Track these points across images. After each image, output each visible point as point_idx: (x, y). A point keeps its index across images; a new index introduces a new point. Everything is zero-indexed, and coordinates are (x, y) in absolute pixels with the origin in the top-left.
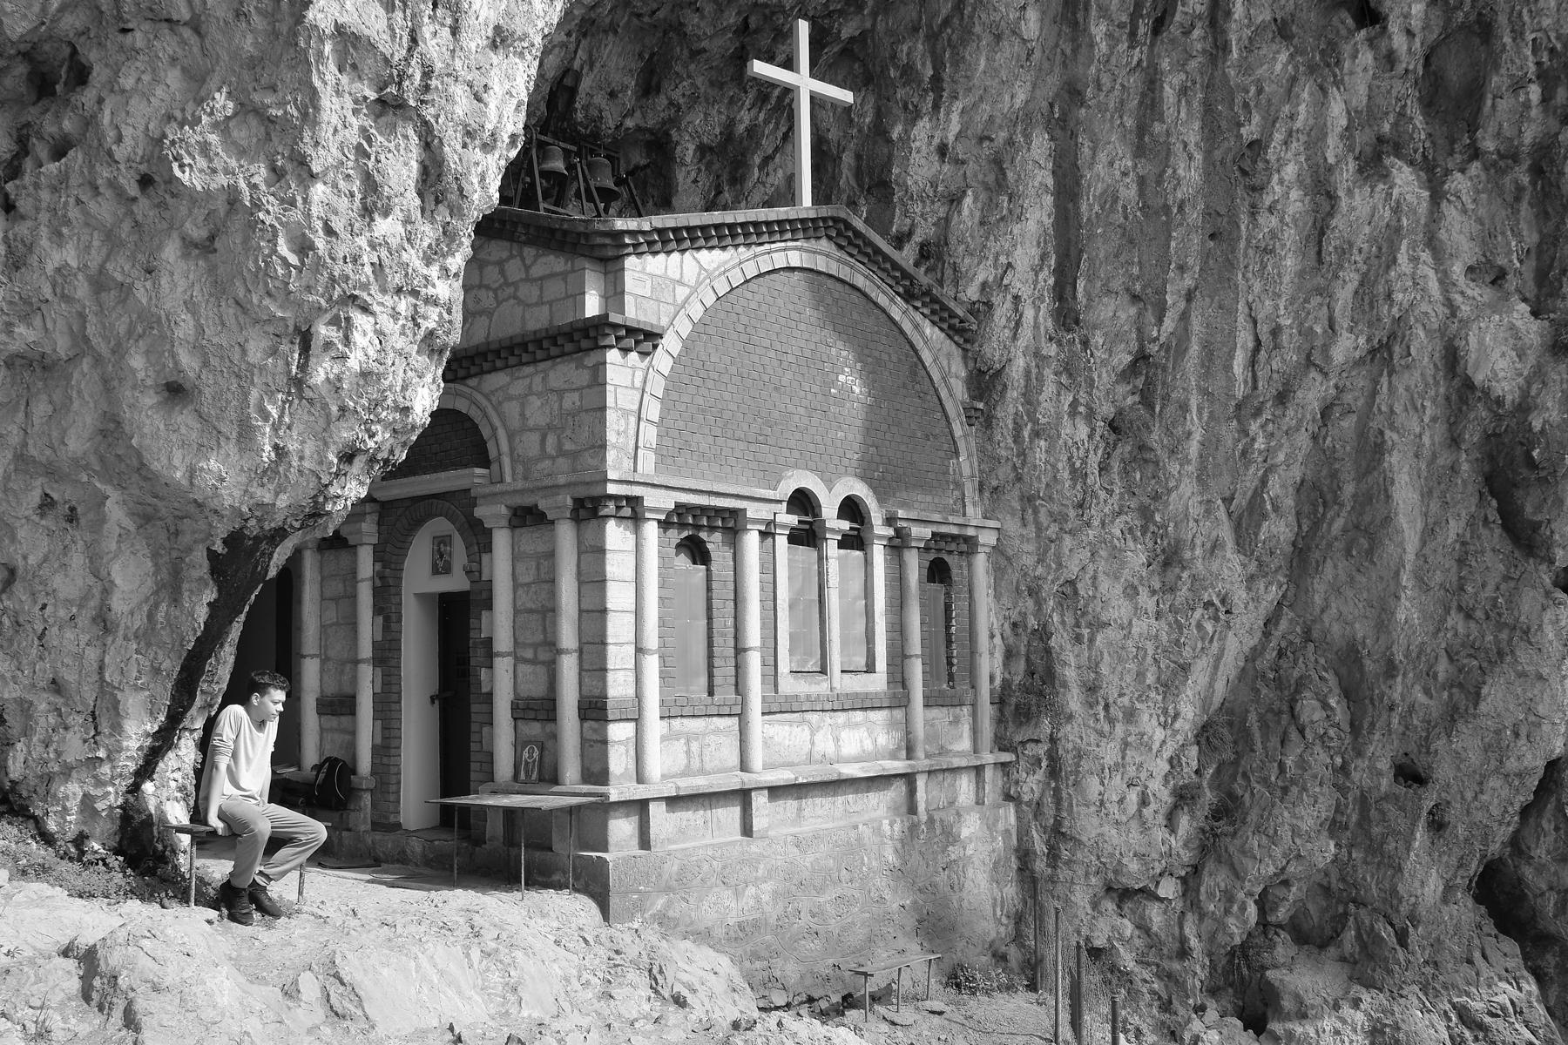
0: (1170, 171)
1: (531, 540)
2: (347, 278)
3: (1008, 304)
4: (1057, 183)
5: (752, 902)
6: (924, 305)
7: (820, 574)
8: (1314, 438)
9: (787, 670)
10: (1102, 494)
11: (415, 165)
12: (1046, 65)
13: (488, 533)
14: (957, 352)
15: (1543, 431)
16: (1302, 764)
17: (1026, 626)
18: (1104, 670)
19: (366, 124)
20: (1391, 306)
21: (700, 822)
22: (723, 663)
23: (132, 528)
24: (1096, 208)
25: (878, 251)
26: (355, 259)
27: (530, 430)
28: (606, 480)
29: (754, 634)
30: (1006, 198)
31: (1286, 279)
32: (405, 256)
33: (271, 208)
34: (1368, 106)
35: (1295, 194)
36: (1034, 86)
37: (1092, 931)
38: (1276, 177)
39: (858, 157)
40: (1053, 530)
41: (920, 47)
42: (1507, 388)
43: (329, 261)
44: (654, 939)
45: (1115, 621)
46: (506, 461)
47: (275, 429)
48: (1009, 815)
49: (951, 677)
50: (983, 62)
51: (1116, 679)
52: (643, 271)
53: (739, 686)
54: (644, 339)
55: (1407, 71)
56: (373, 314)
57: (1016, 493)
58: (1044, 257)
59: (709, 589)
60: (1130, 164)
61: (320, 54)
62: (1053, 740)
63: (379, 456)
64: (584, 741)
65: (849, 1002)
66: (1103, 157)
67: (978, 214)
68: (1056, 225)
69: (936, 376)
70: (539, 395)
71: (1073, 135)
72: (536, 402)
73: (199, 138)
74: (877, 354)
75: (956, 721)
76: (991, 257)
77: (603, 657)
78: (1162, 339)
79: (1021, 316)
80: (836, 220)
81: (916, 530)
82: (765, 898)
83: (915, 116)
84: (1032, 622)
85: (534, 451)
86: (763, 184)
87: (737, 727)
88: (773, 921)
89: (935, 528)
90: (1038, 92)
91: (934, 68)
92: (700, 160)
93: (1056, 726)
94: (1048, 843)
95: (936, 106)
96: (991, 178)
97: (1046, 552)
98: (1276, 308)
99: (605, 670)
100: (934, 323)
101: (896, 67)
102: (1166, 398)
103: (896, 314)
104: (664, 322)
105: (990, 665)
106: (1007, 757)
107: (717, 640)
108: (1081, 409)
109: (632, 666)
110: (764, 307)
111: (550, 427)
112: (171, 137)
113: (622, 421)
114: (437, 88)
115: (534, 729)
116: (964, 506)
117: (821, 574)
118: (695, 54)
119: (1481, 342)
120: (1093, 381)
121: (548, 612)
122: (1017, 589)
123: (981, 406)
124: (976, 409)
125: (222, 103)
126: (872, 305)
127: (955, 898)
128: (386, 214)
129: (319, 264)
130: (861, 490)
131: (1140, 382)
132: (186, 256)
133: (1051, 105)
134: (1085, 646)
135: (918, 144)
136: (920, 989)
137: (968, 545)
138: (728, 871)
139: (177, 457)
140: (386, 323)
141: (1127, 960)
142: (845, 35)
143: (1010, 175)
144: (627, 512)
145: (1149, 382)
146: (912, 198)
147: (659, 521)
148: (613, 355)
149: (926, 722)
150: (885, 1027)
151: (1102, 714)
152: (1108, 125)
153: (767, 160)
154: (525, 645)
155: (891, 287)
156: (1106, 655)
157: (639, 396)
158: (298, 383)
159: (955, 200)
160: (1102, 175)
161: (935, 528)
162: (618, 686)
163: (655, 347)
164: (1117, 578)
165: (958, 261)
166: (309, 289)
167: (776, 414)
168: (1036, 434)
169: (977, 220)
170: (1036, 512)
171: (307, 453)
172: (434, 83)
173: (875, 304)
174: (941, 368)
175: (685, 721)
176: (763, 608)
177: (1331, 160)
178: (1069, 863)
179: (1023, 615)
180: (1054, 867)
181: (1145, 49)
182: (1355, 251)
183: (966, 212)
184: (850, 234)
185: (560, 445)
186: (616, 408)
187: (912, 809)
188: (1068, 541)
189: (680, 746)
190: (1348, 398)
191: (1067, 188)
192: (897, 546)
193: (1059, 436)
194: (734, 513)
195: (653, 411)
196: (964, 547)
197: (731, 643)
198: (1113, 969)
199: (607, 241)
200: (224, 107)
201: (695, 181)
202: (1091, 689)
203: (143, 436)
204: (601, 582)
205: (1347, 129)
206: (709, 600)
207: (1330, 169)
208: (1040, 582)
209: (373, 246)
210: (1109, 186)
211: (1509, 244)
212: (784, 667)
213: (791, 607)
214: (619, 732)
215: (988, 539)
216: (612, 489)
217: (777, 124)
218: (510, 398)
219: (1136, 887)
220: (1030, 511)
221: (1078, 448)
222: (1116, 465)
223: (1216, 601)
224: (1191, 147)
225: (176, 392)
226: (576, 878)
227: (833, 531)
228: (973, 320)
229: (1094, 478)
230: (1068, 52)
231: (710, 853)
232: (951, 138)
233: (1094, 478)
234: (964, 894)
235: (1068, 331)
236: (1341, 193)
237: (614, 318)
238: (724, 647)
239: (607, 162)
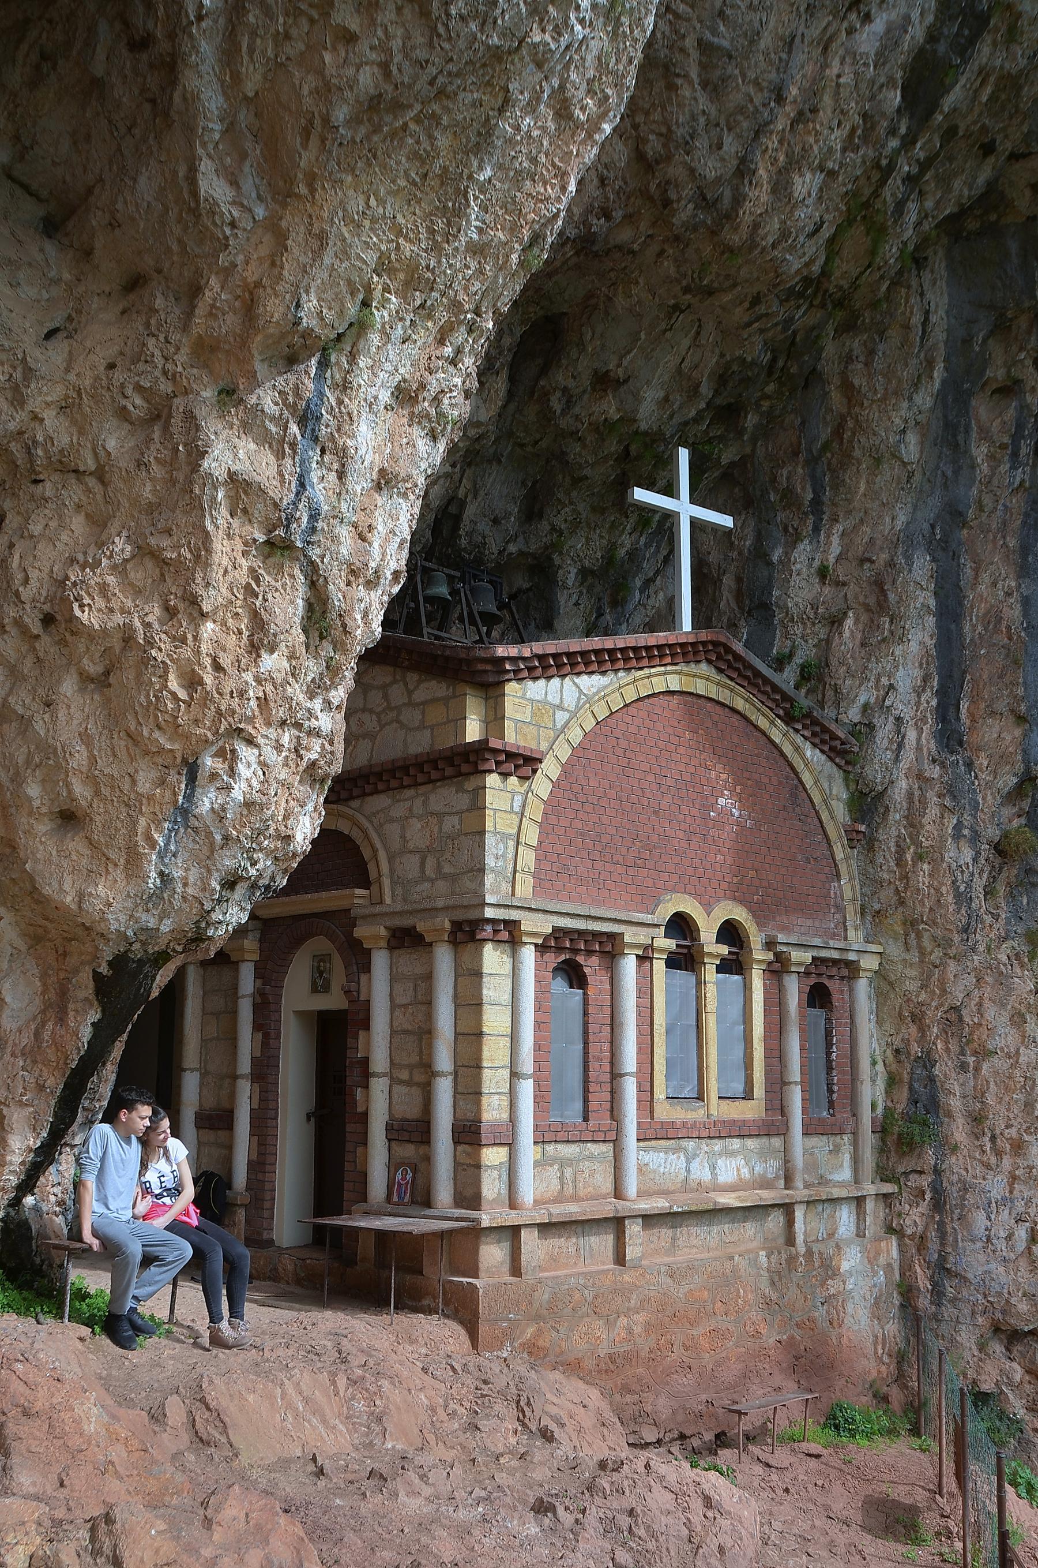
1: (409, 962)
2: (234, 712)
3: (890, 726)
4: (940, 604)
5: (623, 1334)
6: (805, 727)
7: (698, 999)
9: (662, 1097)
10: (988, 919)
11: (300, 602)
13: (368, 953)
14: (838, 774)
17: (909, 1053)
18: (990, 1100)
19: (255, 565)
21: (572, 1250)
22: (598, 1089)
23: (23, 948)
24: (980, 628)
25: (757, 674)
27: (410, 852)
28: (484, 904)
29: (630, 1061)
30: (888, 620)
32: (289, 689)
33: (163, 646)
36: (915, 507)
37: (979, 1374)
39: (739, 580)
40: (937, 955)
41: (800, 471)
43: (216, 696)
44: (523, 1370)
45: (1002, 1049)
46: (386, 882)
47: (161, 856)
48: (892, 1249)
49: (831, 1104)
50: (863, 486)
51: (1003, 1110)
53: (615, 1111)
56: (257, 746)
57: (899, 917)
58: (926, 679)
59: (586, 1013)
60: (1013, 584)
62: (937, 1172)
63: (261, 883)
64: (457, 1164)
65: (722, 1440)
66: (985, 578)
67: (859, 635)
69: (817, 799)
70: (419, 818)
71: (955, 556)
72: (416, 825)
73: (99, 580)
75: (836, 1150)
76: (872, 679)
77: (478, 1080)
79: (903, 737)
80: (716, 644)
81: (796, 955)
82: (637, 1329)
83: (796, 538)
84: (916, 1049)
85: (414, 872)
86: (644, 606)
87: (611, 1154)
88: (644, 1354)
89: (815, 954)
90: (919, 514)
91: (814, 491)
92: (582, 584)
93: (941, 1157)
94: (931, 1279)
95: (816, 529)
96: (872, 601)
97: (929, 977)
99: (479, 1094)
100: (814, 745)
103: (776, 736)
104: (544, 746)
106: (889, 1188)
107: (593, 1065)
108: (966, 832)
109: (507, 1090)
110: (643, 731)
111: (429, 849)
112: (73, 578)
113: (501, 845)
114: (323, 529)
115: (408, 1151)
116: (846, 930)
117: (699, 999)
118: (577, 481)
121: (426, 1033)
122: (900, 1014)
124: (858, 832)
125: (122, 547)
126: (752, 728)
127: (833, 1334)
128: (272, 651)
129: (207, 699)
130: (740, 914)
131: (1026, 804)
132: (82, 690)
133: (933, 526)
134: (970, 1075)
135: (798, 566)
136: (797, 1430)
137: (850, 970)
138: (600, 1300)
139: (68, 880)
140: (270, 755)
141: (1017, 1407)
142: (725, 461)
143: (892, 597)
144: (504, 935)
147: (536, 945)
148: (492, 780)
150: (759, 1469)
153: (648, 582)
154: (401, 1066)
155: (771, 709)
156: (992, 1084)
157: (518, 820)
158: (185, 812)
159: (835, 621)
160: (985, 595)
163: (535, 771)
164: (1003, 1005)
165: (839, 682)
166: (196, 722)
167: (655, 838)
168: (919, 858)
169: (858, 642)
170: (919, 936)
171: (191, 880)
172: (320, 525)
173: (756, 727)
174: (822, 791)
175: (559, 1146)
176: (639, 1033)
178: (954, 1301)
179: (907, 1042)
180: (939, 1305)
181: (1028, 469)
183: (847, 634)
184: (730, 657)
185: (439, 868)
186: (495, 833)
187: (790, 1241)
188: (952, 967)
189: (553, 1171)
192: (778, 969)
193: (943, 859)
194: (612, 937)
195: (532, 835)
196: (845, 972)
197: (608, 1069)
198: (1002, 1415)
199: (489, 667)
200: (123, 550)
201: (577, 604)
202: (977, 1119)
203: (36, 861)
204: (477, 1005)
208: (924, 1008)
209: (259, 681)
210: (992, 606)
212: (660, 1094)
213: (668, 1032)
215: (869, 963)
216: (489, 913)
217: (658, 547)
218: (391, 821)
219: (1026, 1329)
220: (913, 935)
221: (962, 872)
222: (1001, 889)
226: (446, 1303)
227: (711, 955)
228: (854, 741)
229: (979, 902)
230: (949, 473)
231: (582, 1282)
232: (832, 560)
233: (979, 902)
234: (844, 1331)
237: (494, 743)
238: (600, 1072)
239: (490, 586)
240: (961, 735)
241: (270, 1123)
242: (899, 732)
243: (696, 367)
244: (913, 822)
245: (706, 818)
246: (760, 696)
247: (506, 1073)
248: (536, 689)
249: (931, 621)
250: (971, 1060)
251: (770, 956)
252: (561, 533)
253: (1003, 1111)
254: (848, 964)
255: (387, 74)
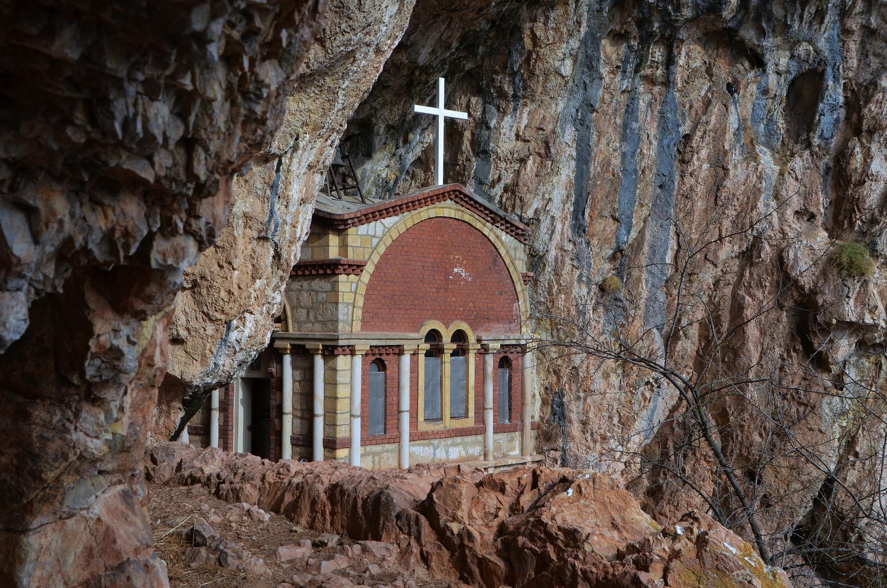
0: (639, 150)
3: (548, 221)
4: (578, 154)
6: (502, 225)
7: (441, 370)
8: (710, 297)
9: (422, 419)
12: (575, 88)
15: (823, 305)
16: (694, 471)
18: (591, 415)
20: (753, 230)
24: (599, 169)
25: (476, 202)
26: (249, 297)
31: (697, 213)
34: (752, 115)
35: (706, 166)
36: (569, 99)
38: (695, 156)
39: (473, 134)
42: (806, 281)
52: (357, 234)
53: (398, 427)
54: (357, 268)
55: (775, 95)
59: (386, 383)
60: (618, 145)
61: (238, 223)
62: (564, 450)
66: (604, 141)
67: (535, 170)
68: (576, 177)
69: (507, 261)
70: (307, 291)
72: (305, 295)
74: (474, 254)
75: (512, 440)
77: (335, 419)
78: (630, 242)
80: (454, 191)
86: (422, 143)
89: (501, 343)
91: (514, 90)
93: (566, 443)
95: (515, 110)
96: (543, 151)
98: (691, 229)
99: (335, 425)
100: (507, 233)
101: (495, 87)
102: (629, 274)
103: (486, 232)
105: (534, 410)
106: (539, 458)
107: (389, 407)
111: (312, 308)
119: (796, 256)
120: (591, 264)
122: (548, 371)
123: (532, 274)
130: (464, 327)
133: (577, 111)
135: (504, 130)
139: (176, 366)
140: (258, 316)
142: (466, 68)
143: (553, 150)
145: (621, 265)
146: (500, 159)
149: (495, 441)
151: (589, 438)
152: (607, 123)
153: (424, 130)
159: (523, 161)
161: (501, 343)
162: (341, 433)
167: (421, 294)
170: (558, 330)
172: (279, 229)
174: (510, 257)
177: (727, 147)
179: (551, 384)
182: (735, 200)
183: (528, 169)
184: (462, 196)
185: (316, 317)
186: (343, 303)
190: (728, 277)
191: (583, 158)
195: (360, 302)
197: (396, 408)
202: (584, 423)
205: (738, 129)
206: (386, 388)
207: (726, 153)
211: (818, 199)
212: (421, 418)
214: (341, 453)
216: (341, 343)
223: (651, 380)
224: (652, 138)
225: (176, 341)
232: (523, 127)
233: (590, 314)
235: (580, 236)
236: (730, 167)
237: (344, 260)
240: (585, 227)
241: (230, 433)
242: (552, 224)
243: (450, 37)
244: (557, 274)
245: (447, 279)
246: (478, 212)
247: (348, 415)
248: (363, 229)
249: (573, 163)
250: (582, 395)
251: (479, 346)
252: (376, 110)
253: (597, 421)
254: (519, 345)
255: (308, 67)
